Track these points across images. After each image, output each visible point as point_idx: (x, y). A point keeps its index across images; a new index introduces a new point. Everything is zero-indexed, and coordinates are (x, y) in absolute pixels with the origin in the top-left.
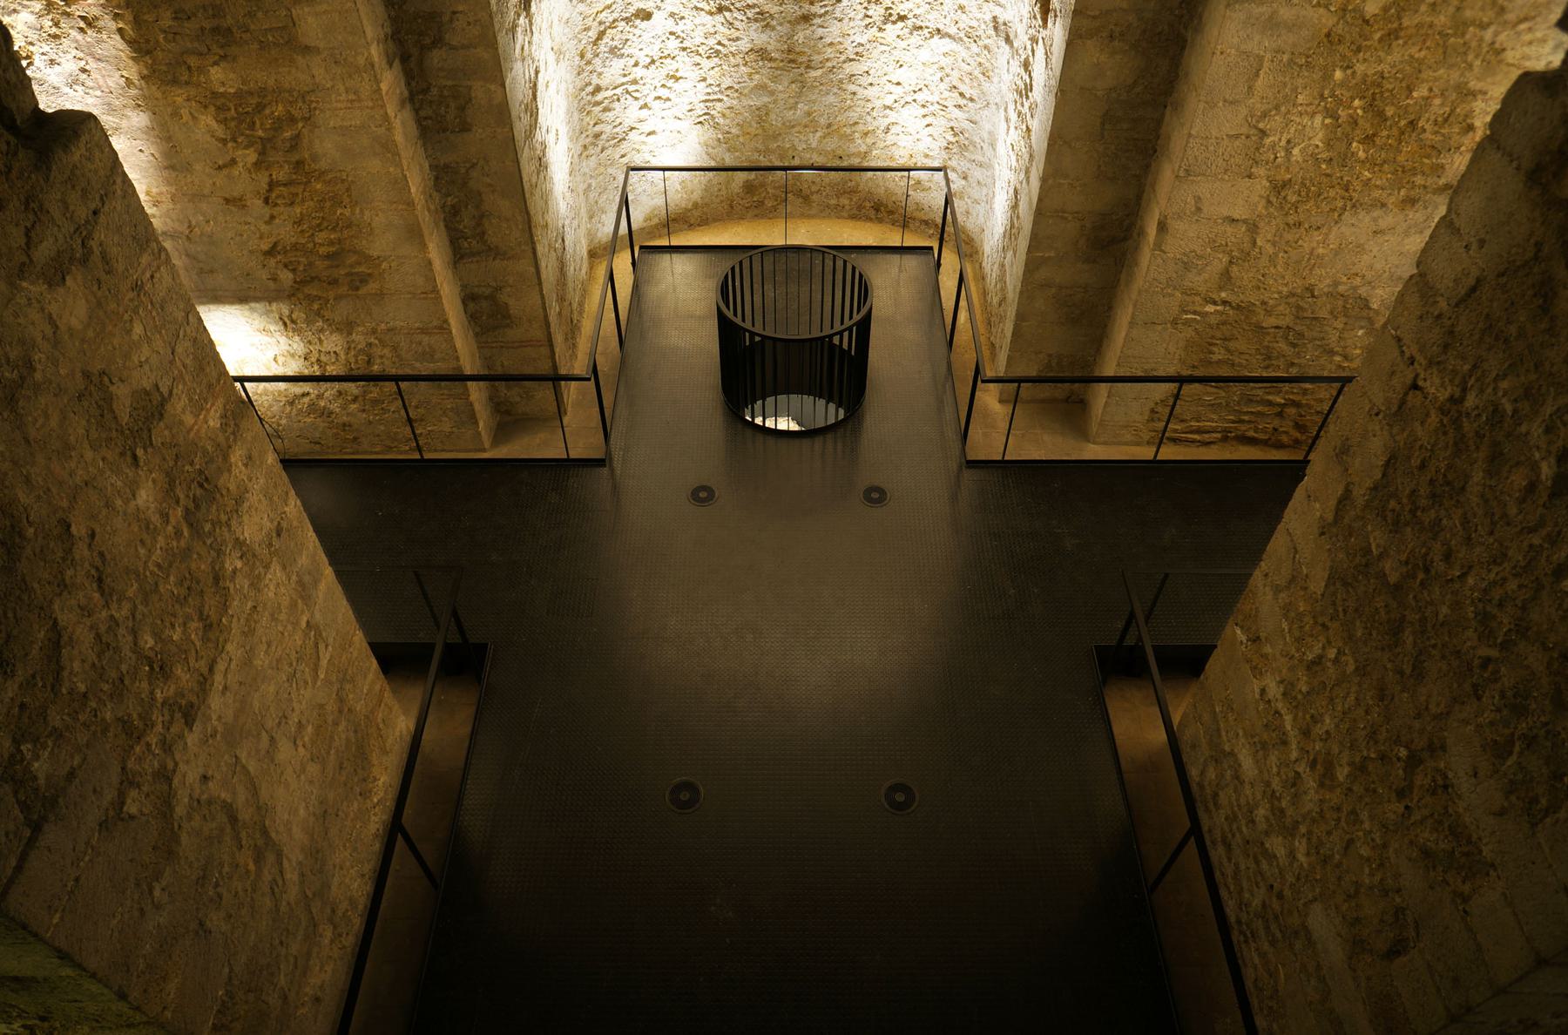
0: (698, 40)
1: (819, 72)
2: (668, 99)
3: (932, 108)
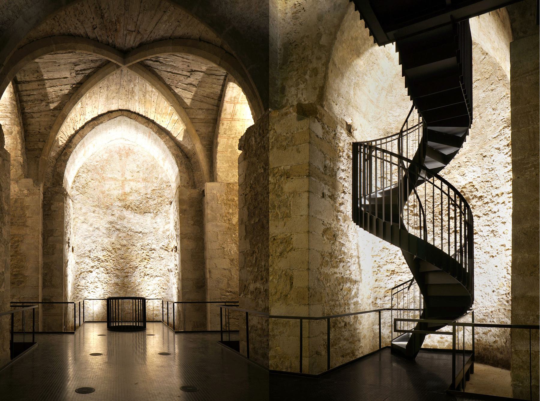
0: (103, 279)
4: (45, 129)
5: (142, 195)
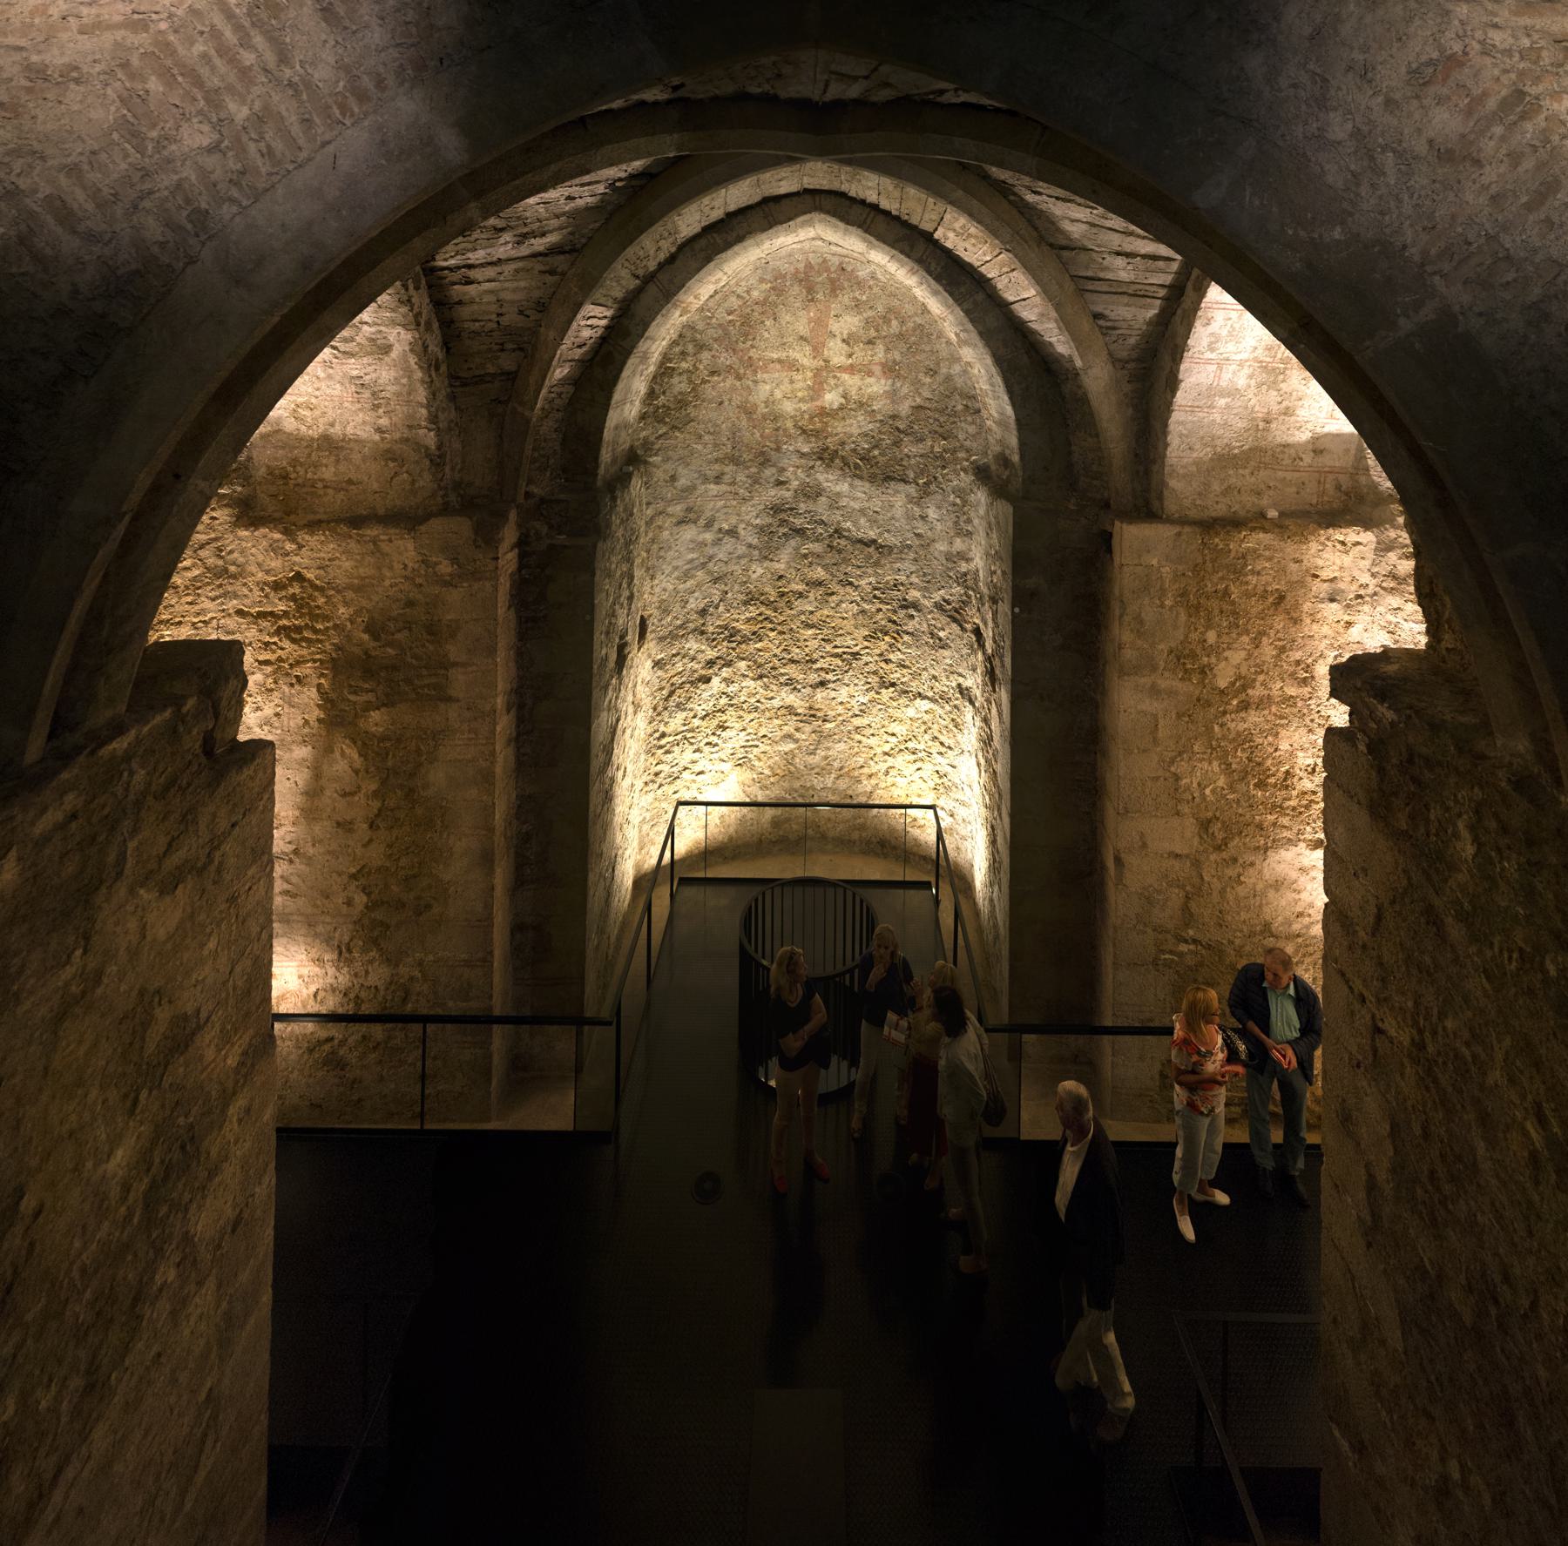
0: (742, 699)
1: (832, 725)
2: (716, 745)
3: (920, 755)
4: (521, 313)
5: (879, 417)
